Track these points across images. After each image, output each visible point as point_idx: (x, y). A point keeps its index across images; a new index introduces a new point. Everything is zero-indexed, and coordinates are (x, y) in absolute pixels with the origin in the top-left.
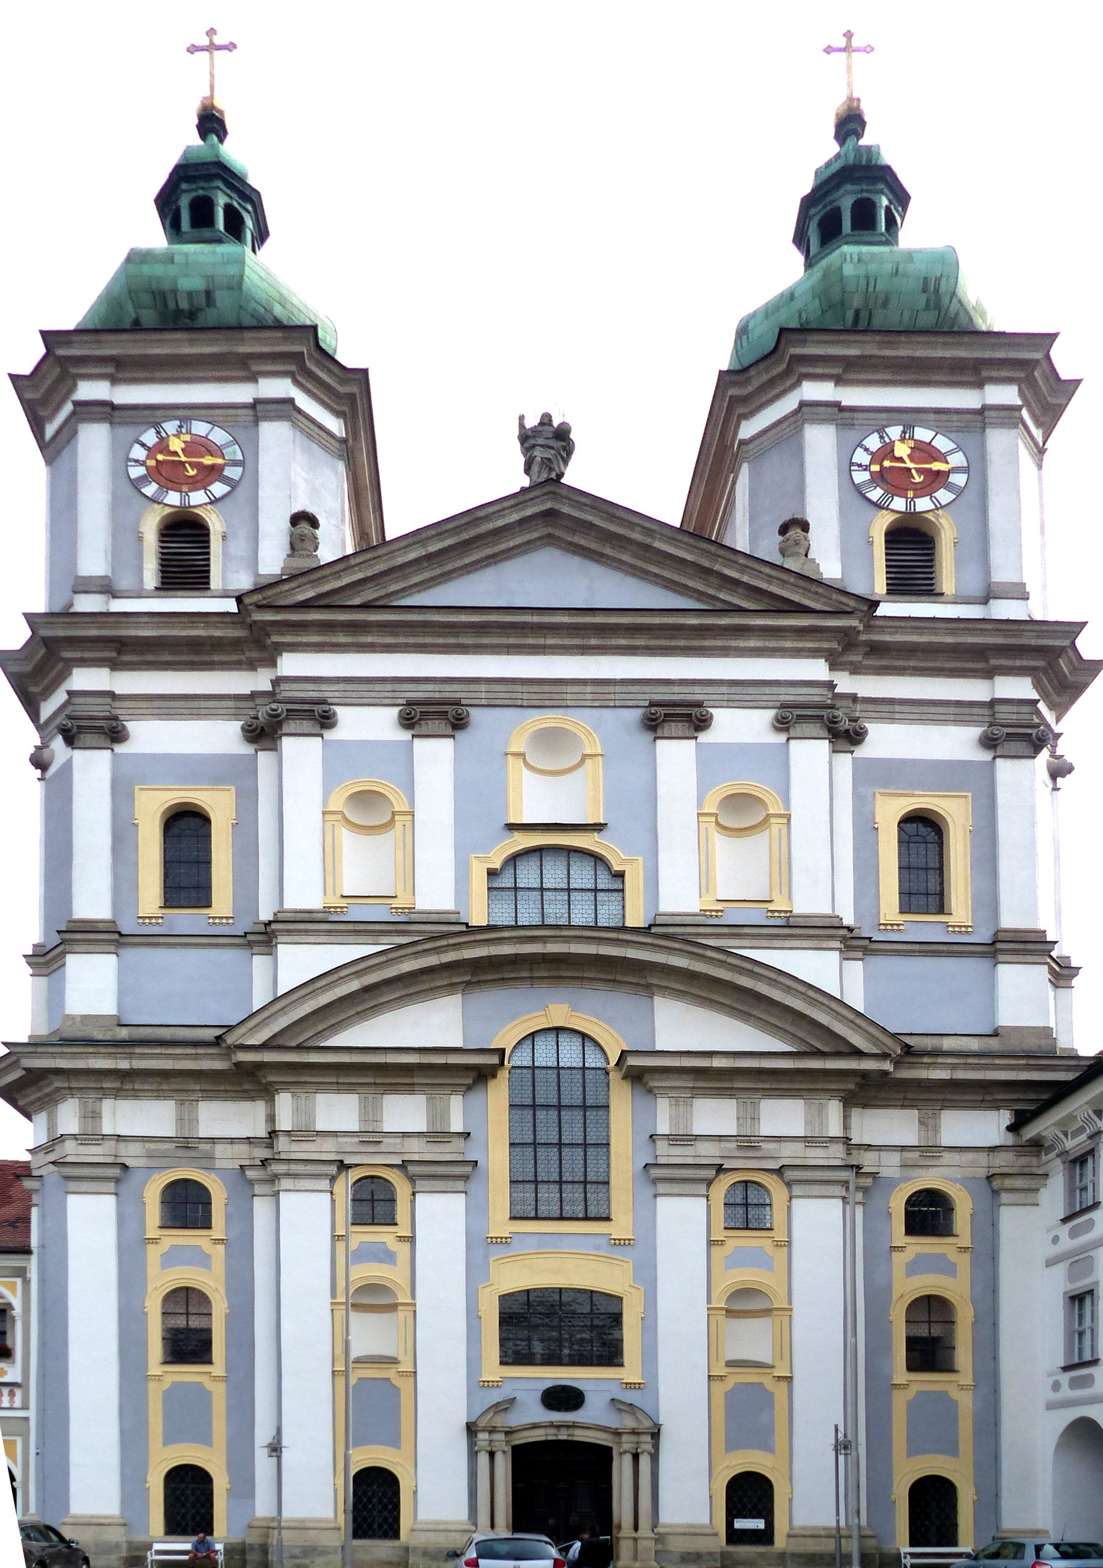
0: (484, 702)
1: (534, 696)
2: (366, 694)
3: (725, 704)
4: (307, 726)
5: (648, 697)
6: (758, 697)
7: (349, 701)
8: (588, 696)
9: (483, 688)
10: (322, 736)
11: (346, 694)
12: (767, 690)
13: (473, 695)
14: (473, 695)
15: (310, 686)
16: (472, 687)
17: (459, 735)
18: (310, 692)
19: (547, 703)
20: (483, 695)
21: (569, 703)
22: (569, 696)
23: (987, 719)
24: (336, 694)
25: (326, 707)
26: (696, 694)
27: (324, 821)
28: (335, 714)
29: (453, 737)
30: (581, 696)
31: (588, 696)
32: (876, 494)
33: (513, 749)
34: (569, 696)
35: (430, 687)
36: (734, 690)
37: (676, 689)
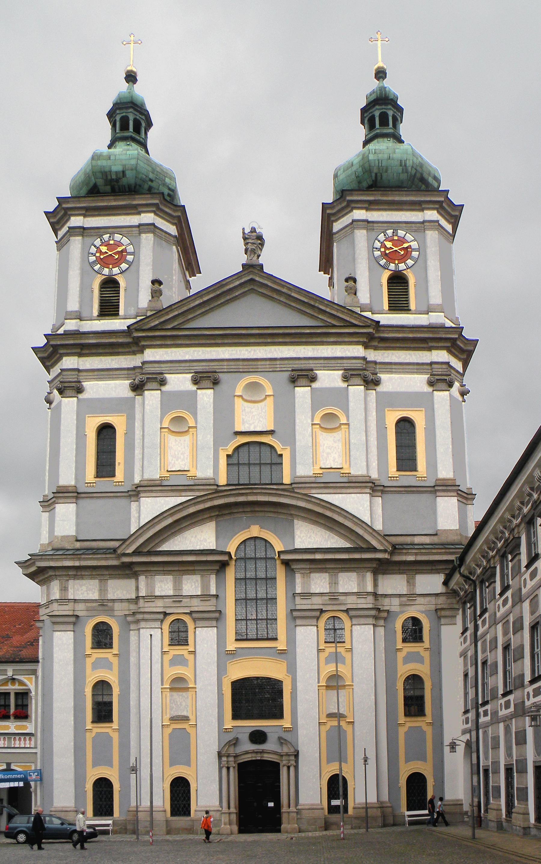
0: (225, 370)
1: (246, 367)
2: (179, 368)
3: (322, 368)
4: (155, 385)
5: (291, 366)
6: (336, 365)
7: (171, 372)
8: (268, 366)
9: (225, 363)
10: (160, 390)
11: (171, 368)
12: (339, 361)
13: (222, 367)
14: (222, 367)
15: (156, 365)
16: (221, 363)
17: (217, 388)
18: (156, 368)
19: (251, 370)
20: (225, 367)
21: (259, 370)
22: (259, 367)
23: (430, 371)
24: (167, 369)
25: (161, 376)
26: (311, 364)
27: (161, 432)
28: (166, 378)
29: (213, 388)
30: (264, 366)
31: (268, 366)
32: (383, 262)
33: (236, 394)
34: (259, 367)
35: (204, 364)
36: (326, 361)
37: (303, 362)
